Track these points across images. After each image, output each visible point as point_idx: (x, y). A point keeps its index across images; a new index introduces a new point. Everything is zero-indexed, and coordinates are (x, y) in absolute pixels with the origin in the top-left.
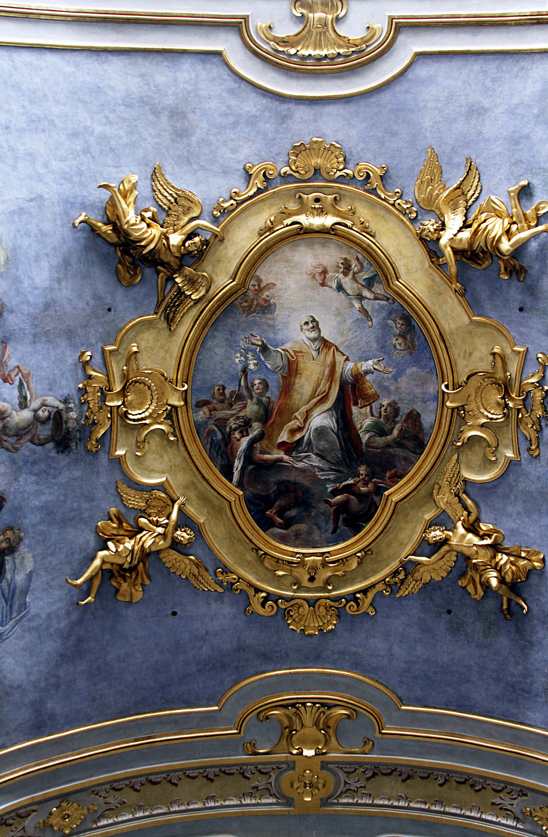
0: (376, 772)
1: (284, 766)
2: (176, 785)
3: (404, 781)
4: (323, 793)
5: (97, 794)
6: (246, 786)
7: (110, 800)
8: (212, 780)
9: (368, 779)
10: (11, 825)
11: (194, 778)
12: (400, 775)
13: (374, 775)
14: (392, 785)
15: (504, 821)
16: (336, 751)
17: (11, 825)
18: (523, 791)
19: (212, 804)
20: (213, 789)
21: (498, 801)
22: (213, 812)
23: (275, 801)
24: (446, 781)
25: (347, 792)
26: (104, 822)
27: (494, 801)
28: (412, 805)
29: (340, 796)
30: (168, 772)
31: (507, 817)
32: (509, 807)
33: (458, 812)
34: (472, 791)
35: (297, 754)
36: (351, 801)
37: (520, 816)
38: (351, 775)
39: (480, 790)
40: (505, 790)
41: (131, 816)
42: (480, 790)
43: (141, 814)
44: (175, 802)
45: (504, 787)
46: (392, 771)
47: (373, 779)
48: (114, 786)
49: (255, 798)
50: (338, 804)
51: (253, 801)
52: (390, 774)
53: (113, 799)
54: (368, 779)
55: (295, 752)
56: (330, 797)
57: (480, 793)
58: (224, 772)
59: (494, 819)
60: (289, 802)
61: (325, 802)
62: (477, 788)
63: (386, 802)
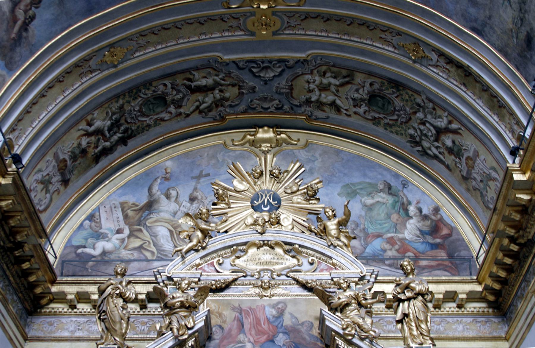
0: (307, 16)
1: (249, 14)
2: (180, 29)
3: (325, 22)
4: (274, 29)
5: (132, 40)
6: (225, 26)
7: (140, 41)
8: (203, 24)
9: (302, 20)
10: (81, 66)
11: (191, 24)
12: (323, 18)
13: (306, 18)
14: (318, 24)
15: (386, 48)
16: (282, 5)
17: (81, 66)
18: (399, 33)
19: (204, 37)
20: (204, 29)
21: (383, 36)
22: (205, 42)
23: (243, 33)
24: (351, 23)
25: (289, 27)
26: (138, 54)
27: (381, 36)
28: (330, 35)
29: (285, 29)
30: (175, 22)
31: (388, 45)
32: (390, 41)
33: (359, 40)
34: (368, 30)
35: (256, 8)
36: (291, 32)
37: (397, 46)
38: (291, 18)
39: (372, 29)
40: (388, 31)
41: (154, 49)
42: (372, 29)
43: (160, 47)
44: (181, 38)
45: (387, 30)
46: (318, 16)
47: (305, 21)
48: (142, 34)
49: (231, 32)
50: (284, 34)
51: (230, 34)
52: (316, 17)
53: (142, 41)
54: (302, 20)
55: (255, 6)
56: (279, 30)
57: (373, 31)
58: (211, 19)
59: (381, 46)
60: (252, 34)
61: (275, 33)
62: (371, 28)
63: (314, 33)
